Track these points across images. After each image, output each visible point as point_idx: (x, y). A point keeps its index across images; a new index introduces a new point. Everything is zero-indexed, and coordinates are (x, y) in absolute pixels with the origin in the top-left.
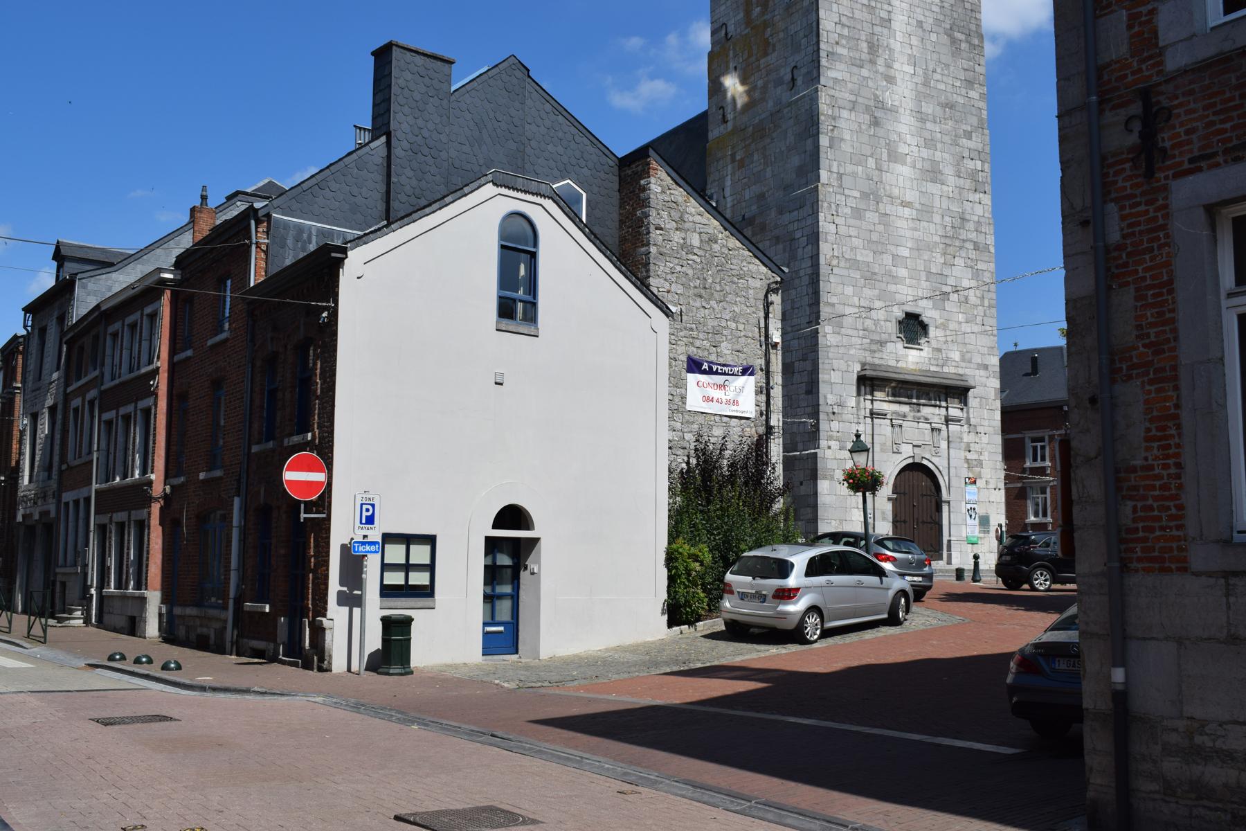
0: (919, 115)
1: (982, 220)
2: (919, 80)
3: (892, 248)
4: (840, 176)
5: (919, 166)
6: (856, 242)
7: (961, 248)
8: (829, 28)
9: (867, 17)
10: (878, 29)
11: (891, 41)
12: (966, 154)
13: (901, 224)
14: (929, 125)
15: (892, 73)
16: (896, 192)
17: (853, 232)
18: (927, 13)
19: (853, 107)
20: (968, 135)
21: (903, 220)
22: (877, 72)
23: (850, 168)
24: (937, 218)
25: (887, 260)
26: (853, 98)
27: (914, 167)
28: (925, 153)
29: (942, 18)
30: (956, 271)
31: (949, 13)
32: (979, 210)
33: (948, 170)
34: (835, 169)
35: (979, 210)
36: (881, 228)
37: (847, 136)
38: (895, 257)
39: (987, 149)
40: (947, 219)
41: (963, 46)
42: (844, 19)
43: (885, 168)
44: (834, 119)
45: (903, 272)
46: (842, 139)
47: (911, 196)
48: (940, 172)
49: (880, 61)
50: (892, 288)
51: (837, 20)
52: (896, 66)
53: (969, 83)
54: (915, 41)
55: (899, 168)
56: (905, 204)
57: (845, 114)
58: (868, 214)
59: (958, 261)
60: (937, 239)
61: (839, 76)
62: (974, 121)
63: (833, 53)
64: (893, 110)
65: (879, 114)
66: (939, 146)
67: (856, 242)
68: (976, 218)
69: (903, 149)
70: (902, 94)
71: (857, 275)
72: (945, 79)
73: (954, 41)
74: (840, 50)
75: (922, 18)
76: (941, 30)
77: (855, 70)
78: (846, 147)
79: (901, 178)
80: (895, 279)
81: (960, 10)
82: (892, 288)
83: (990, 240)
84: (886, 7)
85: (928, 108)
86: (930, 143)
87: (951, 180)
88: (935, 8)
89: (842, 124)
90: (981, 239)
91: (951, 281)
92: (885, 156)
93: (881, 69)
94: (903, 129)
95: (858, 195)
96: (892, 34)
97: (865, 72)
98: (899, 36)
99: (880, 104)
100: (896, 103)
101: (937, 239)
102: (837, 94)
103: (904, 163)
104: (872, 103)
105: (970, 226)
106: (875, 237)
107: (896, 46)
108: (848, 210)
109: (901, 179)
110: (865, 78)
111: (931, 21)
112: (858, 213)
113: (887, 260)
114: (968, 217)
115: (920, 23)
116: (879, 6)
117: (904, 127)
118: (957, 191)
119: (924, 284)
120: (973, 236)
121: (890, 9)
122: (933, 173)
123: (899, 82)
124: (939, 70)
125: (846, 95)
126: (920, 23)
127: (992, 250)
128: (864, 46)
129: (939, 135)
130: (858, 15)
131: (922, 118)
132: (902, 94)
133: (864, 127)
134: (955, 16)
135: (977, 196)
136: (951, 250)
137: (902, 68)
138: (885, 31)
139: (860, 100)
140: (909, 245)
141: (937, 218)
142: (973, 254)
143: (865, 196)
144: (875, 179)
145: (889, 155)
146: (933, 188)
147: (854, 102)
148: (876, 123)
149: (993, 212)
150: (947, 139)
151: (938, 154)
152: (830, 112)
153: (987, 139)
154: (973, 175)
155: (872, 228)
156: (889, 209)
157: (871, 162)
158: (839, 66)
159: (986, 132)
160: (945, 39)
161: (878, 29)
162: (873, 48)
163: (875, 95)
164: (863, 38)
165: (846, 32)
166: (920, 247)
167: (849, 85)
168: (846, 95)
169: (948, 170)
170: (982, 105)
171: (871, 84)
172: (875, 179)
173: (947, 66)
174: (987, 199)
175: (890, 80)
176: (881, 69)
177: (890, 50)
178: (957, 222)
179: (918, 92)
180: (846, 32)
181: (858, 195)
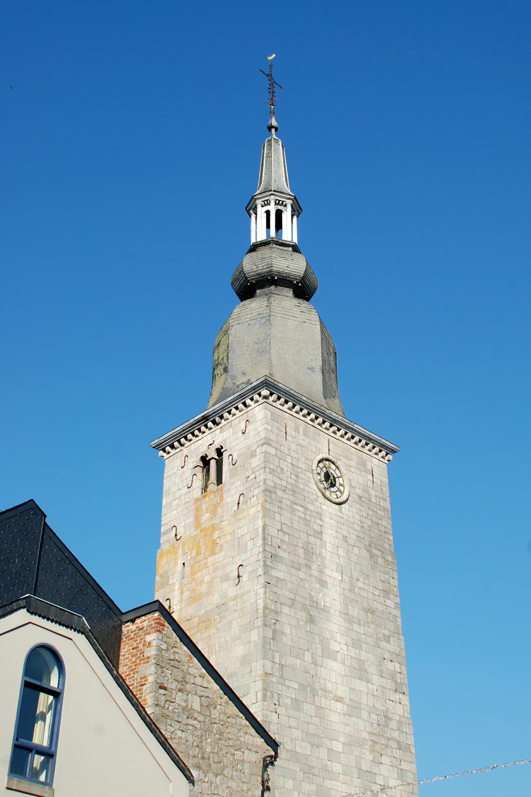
0: (346, 617)
1: (403, 720)
2: (346, 586)
3: (327, 742)
4: (282, 666)
5: (348, 663)
6: (297, 733)
7: (387, 746)
8: (272, 534)
9: (304, 528)
10: (312, 539)
11: (323, 550)
12: (387, 656)
13: (334, 717)
14: (355, 627)
15: (324, 577)
16: (329, 686)
17: (293, 723)
18: (351, 531)
19: (293, 603)
20: (387, 639)
21: (336, 713)
22: (311, 575)
23: (290, 661)
24: (365, 715)
25: (323, 753)
26: (292, 596)
27: (344, 664)
28: (353, 652)
29: (362, 535)
30: (384, 770)
31: (367, 532)
32: (400, 710)
33: (372, 670)
34: (277, 660)
35: (400, 710)
36: (317, 720)
37: (287, 631)
38: (330, 750)
39: (403, 653)
40: (374, 716)
41: (380, 560)
42: (285, 528)
43: (320, 663)
44: (276, 613)
45: (337, 768)
46: (283, 633)
47: (342, 691)
48: (366, 671)
49: (314, 566)
50: (328, 783)
51: (279, 528)
52: (327, 571)
53: (386, 593)
54: (341, 552)
55: (332, 664)
56: (339, 699)
57: (286, 610)
58: (306, 706)
59: (384, 759)
60: (365, 735)
61: (281, 575)
62: (391, 626)
63: (276, 556)
64: (325, 610)
65: (314, 612)
66: (364, 646)
67: (297, 733)
68: (398, 718)
69: (334, 646)
70: (332, 597)
71: (296, 767)
72: (366, 587)
73: (372, 556)
74: (281, 553)
77: (294, 571)
78: (287, 640)
79: (334, 673)
80: (330, 774)
81: (376, 531)
82: (328, 783)
83: (411, 740)
84: (318, 521)
85: (354, 612)
86: (357, 643)
87: (375, 679)
88: (356, 527)
89: (283, 619)
90: (402, 738)
91: (380, 780)
92: (319, 652)
93: (315, 573)
94: (334, 628)
95: (297, 687)
96: (323, 544)
97: (302, 575)
99: (315, 604)
100: (328, 604)
101: (365, 735)
102: (279, 591)
103: (335, 660)
104: (308, 602)
105: (393, 724)
106: (312, 729)
107: (328, 556)
108: (288, 701)
109: (333, 674)
110: (301, 579)
111: (354, 537)
112: (297, 704)
113: (323, 753)
114: (390, 716)
115: (345, 538)
116: (313, 520)
117: (334, 626)
118: (380, 691)
119: (357, 781)
120: (396, 734)
121: (322, 523)
122: (360, 671)
123: (330, 587)
124: (361, 579)
125: (287, 593)
127: (413, 750)
128: (301, 552)
129: (364, 636)
130: (296, 525)
131: (349, 619)
132: (332, 597)
133: (301, 623)
135: (398, 696)
136: (378, 747)
137: (332, 574)
138: (318, 542)
139: (298, 598)
140: (342, 739)
141: (365, 715)
142: (397, 753)
143: (303, 688)
144: (312, 672)
145: (323, 651)
146: (361, 686)
147: (293, 600)
148: (311, 620)
149: (411, 713)
150: (369, 640)
151: (363, 653)
152: (273, 607)
153: (403, 645)
154: (392, 676)
155: (309, 720)
156: (324, 702)
157: (308, 656)
158: (281, 567)
159: (402, 637)
160: (365, 554)
161: (312, 539)
162: (309, 553)
163: (310, 595)
165: (286, 538)
166: (353, 742)
167: (289, 584)
168: (287, 593)
169: (372, 670)
170: (397, 613)
171: (307, 585)
172: (312, 672)
173: (368, 576)
174: (405, 700)
175: (323, 583)
176: (315, 573)
177: (322, 557)
178: (382, 720)
179: (346, 597)
180: (286, 538)
181: (297, 687)
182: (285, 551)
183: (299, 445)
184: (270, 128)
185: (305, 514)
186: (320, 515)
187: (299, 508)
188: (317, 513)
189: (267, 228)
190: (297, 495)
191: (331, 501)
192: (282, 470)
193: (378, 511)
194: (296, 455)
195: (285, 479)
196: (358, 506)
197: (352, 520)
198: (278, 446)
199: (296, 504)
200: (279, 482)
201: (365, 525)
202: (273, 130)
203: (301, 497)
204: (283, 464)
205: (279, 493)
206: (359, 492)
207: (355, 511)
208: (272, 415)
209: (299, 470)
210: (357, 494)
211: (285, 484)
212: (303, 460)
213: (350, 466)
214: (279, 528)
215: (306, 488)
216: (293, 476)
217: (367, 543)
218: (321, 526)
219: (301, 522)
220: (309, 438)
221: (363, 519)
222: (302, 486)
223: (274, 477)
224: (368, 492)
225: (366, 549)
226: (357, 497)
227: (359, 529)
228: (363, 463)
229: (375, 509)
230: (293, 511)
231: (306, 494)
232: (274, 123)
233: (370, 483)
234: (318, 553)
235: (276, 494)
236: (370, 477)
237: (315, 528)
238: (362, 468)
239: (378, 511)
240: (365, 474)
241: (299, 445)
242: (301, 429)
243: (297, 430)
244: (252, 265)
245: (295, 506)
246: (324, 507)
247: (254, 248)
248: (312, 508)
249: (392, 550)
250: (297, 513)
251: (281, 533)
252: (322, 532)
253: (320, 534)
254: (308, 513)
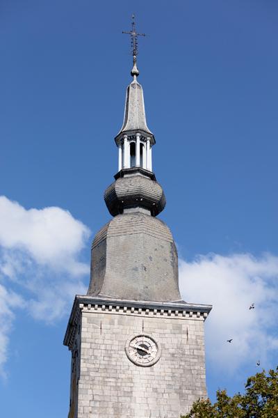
9: (114, 392)
42: (96, 398)
54: (150, 401)
75: (157, 386)
76: (172, 391)
84: (129, 384)
88: (166, 378)
98: (138, 400)
111: (164, 386)
115: (155, 390)
116: (123, 384)
121: (132, 385)
126: (155, 390)
134: (184, 380)
138: (128, 399)
160: (175, 396)
164: (111, 406)
180: (97, 404)
182: (95, 413)
183: (113, 333)
184: (133, 74)
185: (116, 383)
186: (131, 380)
187: (110, 380)
188: (129, 378)
189: (131, 154)
190: (109, 371)
191: (142, 366)
192: (96, 357)
193: (192, 360)
194: (110, 342)
195: (98, 362)
196: (169, 362)
197: (163, 374)
198: (93, 341)
199: (108, 378)
200: (93, 366)
201: (176, 375)
202: (135, 76)
203: (113, 371)
204: (97, 353)
205: (92, 374)
206: (172, 351)
207: (167, 366)
208: (88, 320)
209: (112, 352)
210: (169, 353)
211: (97, 366)
212: (117, 343)
213: (165, 334)
214: (91, 399)
215: (118, 363)
216: (106, 358)
217: (178, 387)
218: (131, 387)
219: (112, 389)
220: (123, 325)
221: (174, 371)
222: (114, 363)
223: (88, 365)
224: (182, 349)
225: (176, 392)
226: (169, 355)
227: (170, 379)
228: (179, 328)
229: (188, 359)
230: (105, 383)
231: (119, 368)
232: (135, 69)
233: (184, 341)
234: (127, 407)
235: (89, 375)
236: (185, 336)
237: (125, 390)
238: (178, 331)
239: (192, 360)
240: (179, 335)
241: (113, 333)
242: (116, 321)
243: (112, 323)
244: (123, 188)
245: (106, 380)
246: (135, 372)
247: (120, 175)
248: (123, 376)
249: (205, 385)
250: (109, 384)
251: (92, 403)
252: (131, 392)
253: (129, 394)
254: (120, 380)
